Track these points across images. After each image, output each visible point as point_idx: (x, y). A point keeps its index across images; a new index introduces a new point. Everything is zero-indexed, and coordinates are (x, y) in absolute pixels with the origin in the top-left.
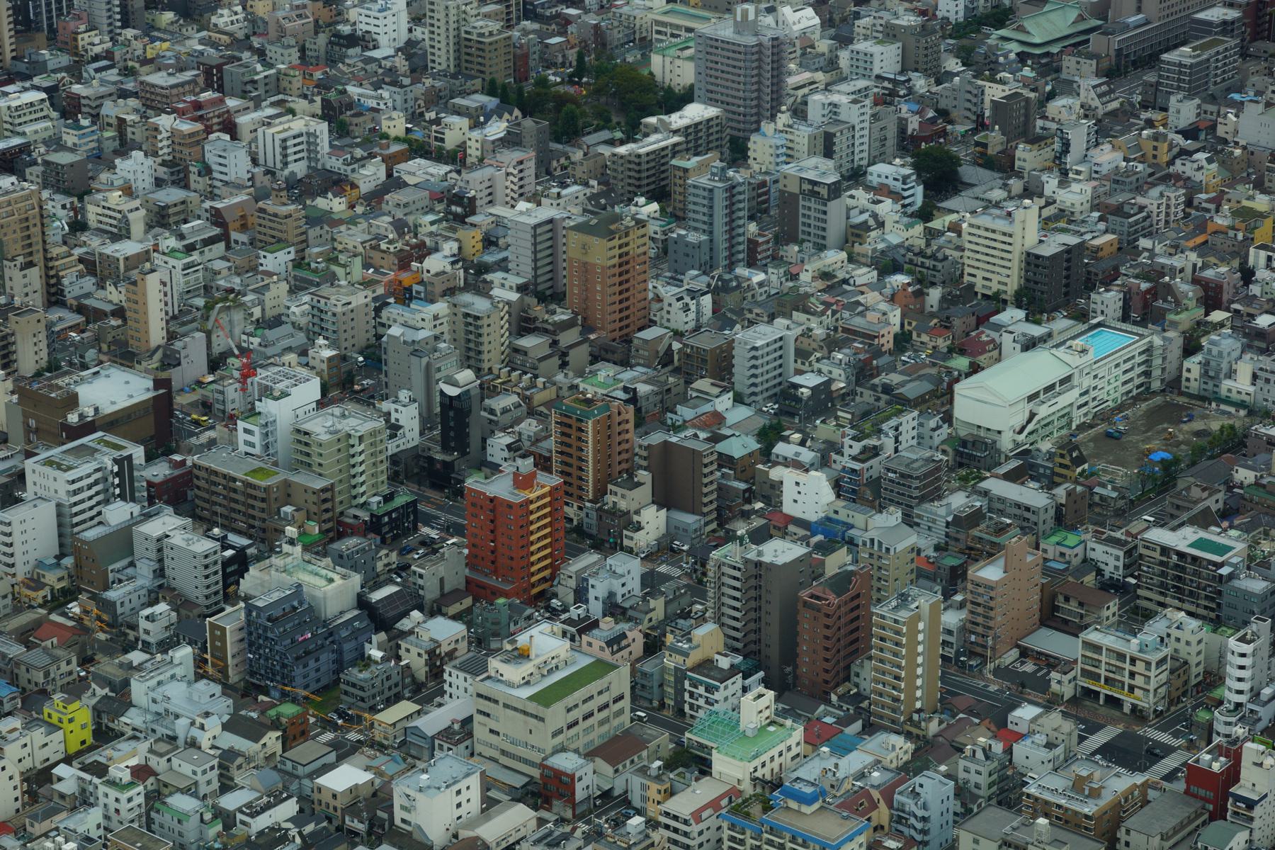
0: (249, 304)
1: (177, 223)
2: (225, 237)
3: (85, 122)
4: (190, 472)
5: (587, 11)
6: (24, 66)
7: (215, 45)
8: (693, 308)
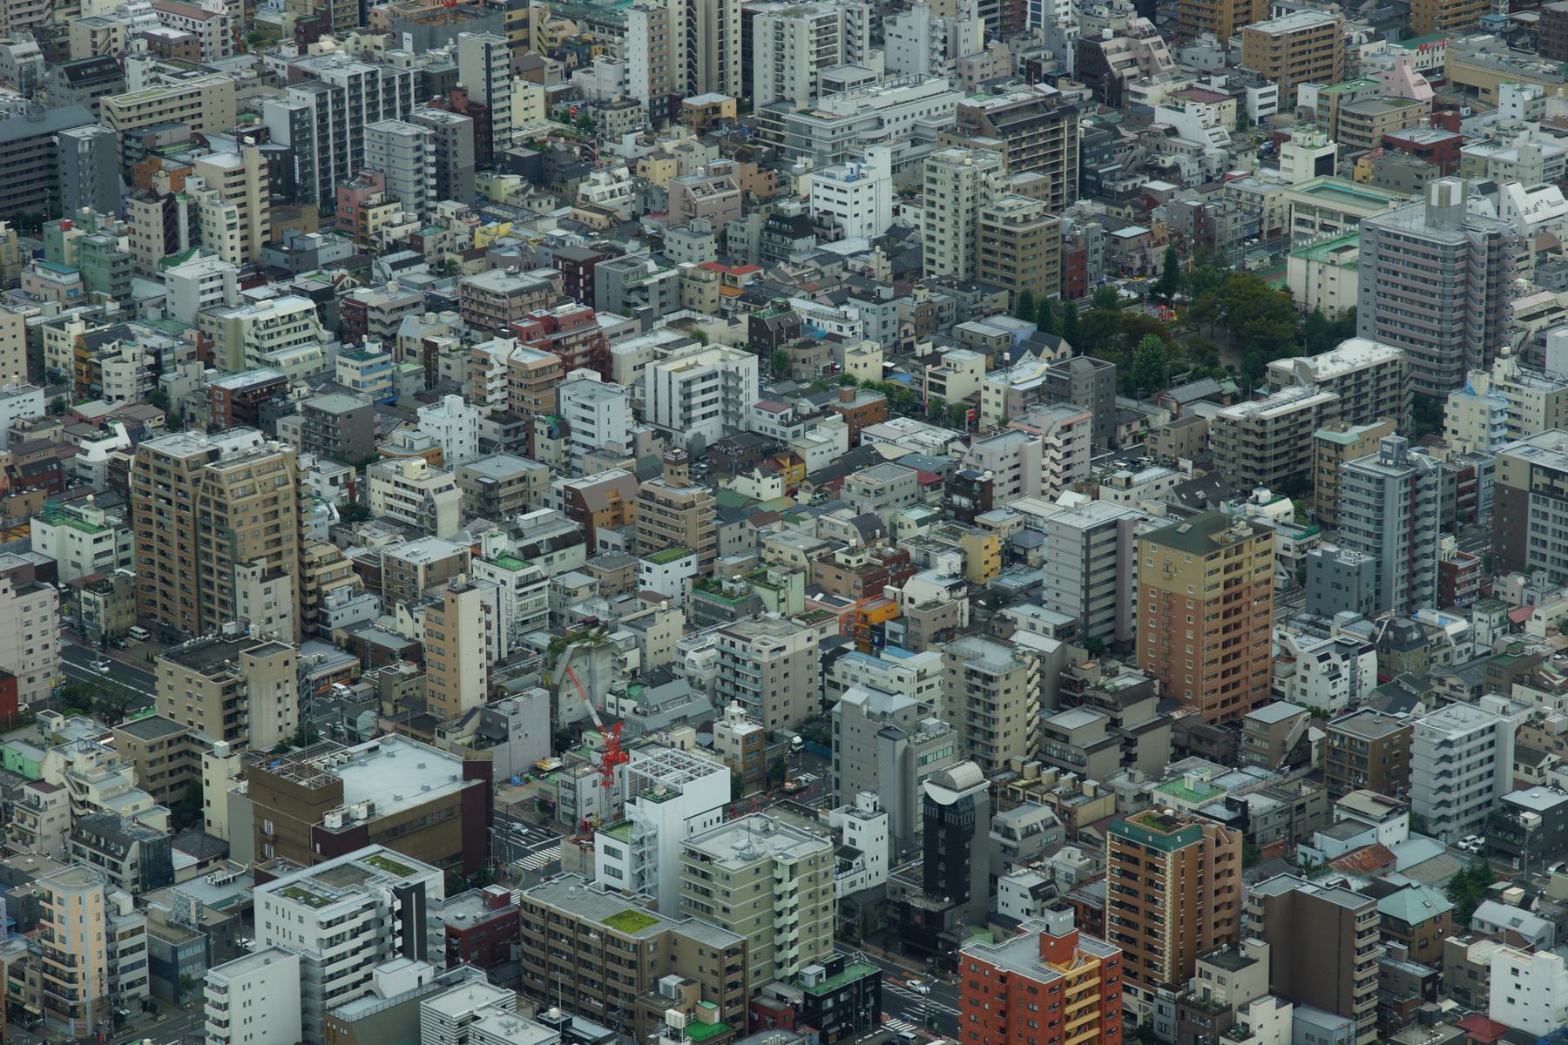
0: (621, 645)
1: (511, 512)
2: (585, 536)
3: (373, 348)
4: (517, 915)
5: (1184, 186)
6: (282, 256)
7: (583, 229)
8: (1345, 673)
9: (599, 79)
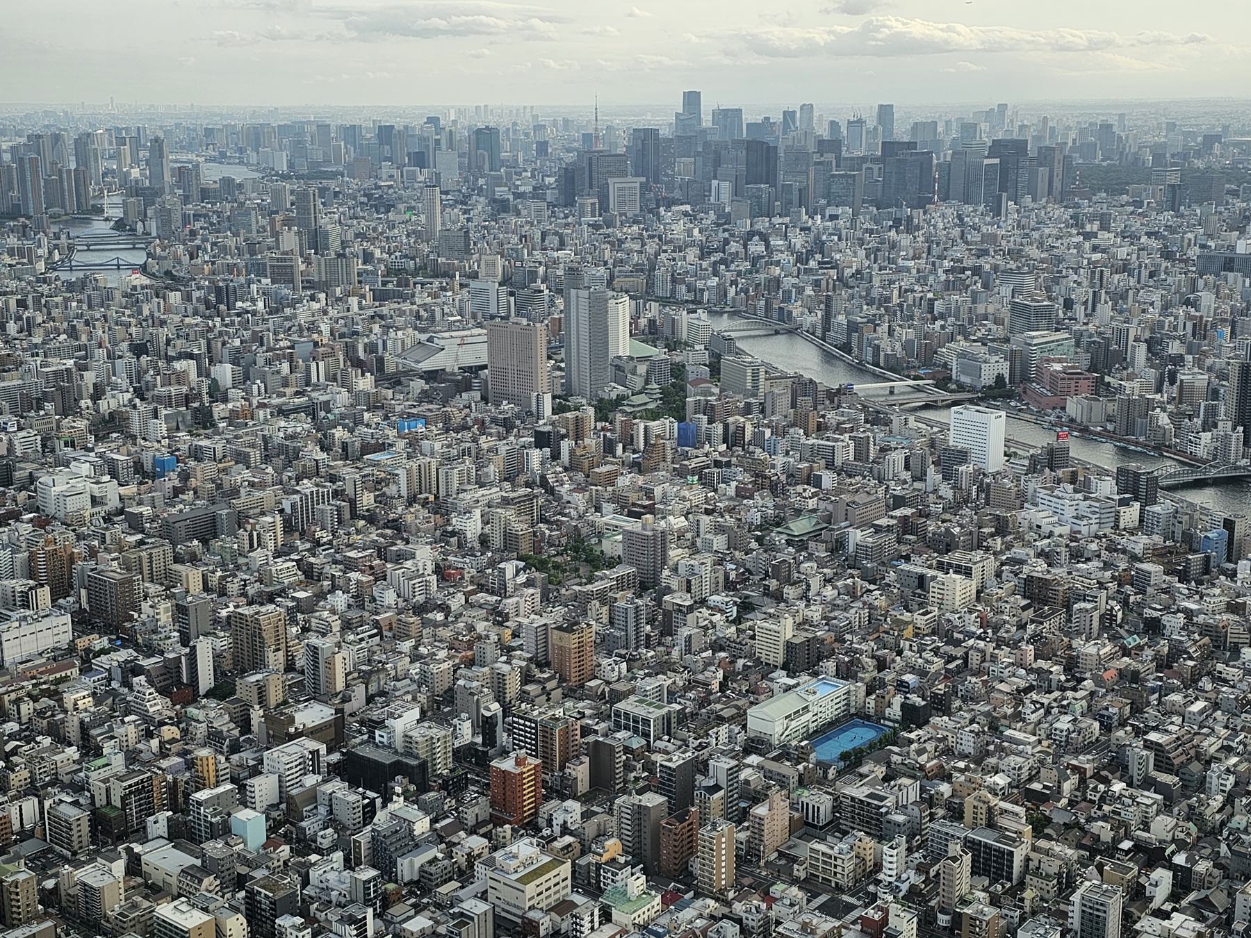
1: (357, 627)
2: (380, 633)
8: (617, 669)
9: (391, 490)
